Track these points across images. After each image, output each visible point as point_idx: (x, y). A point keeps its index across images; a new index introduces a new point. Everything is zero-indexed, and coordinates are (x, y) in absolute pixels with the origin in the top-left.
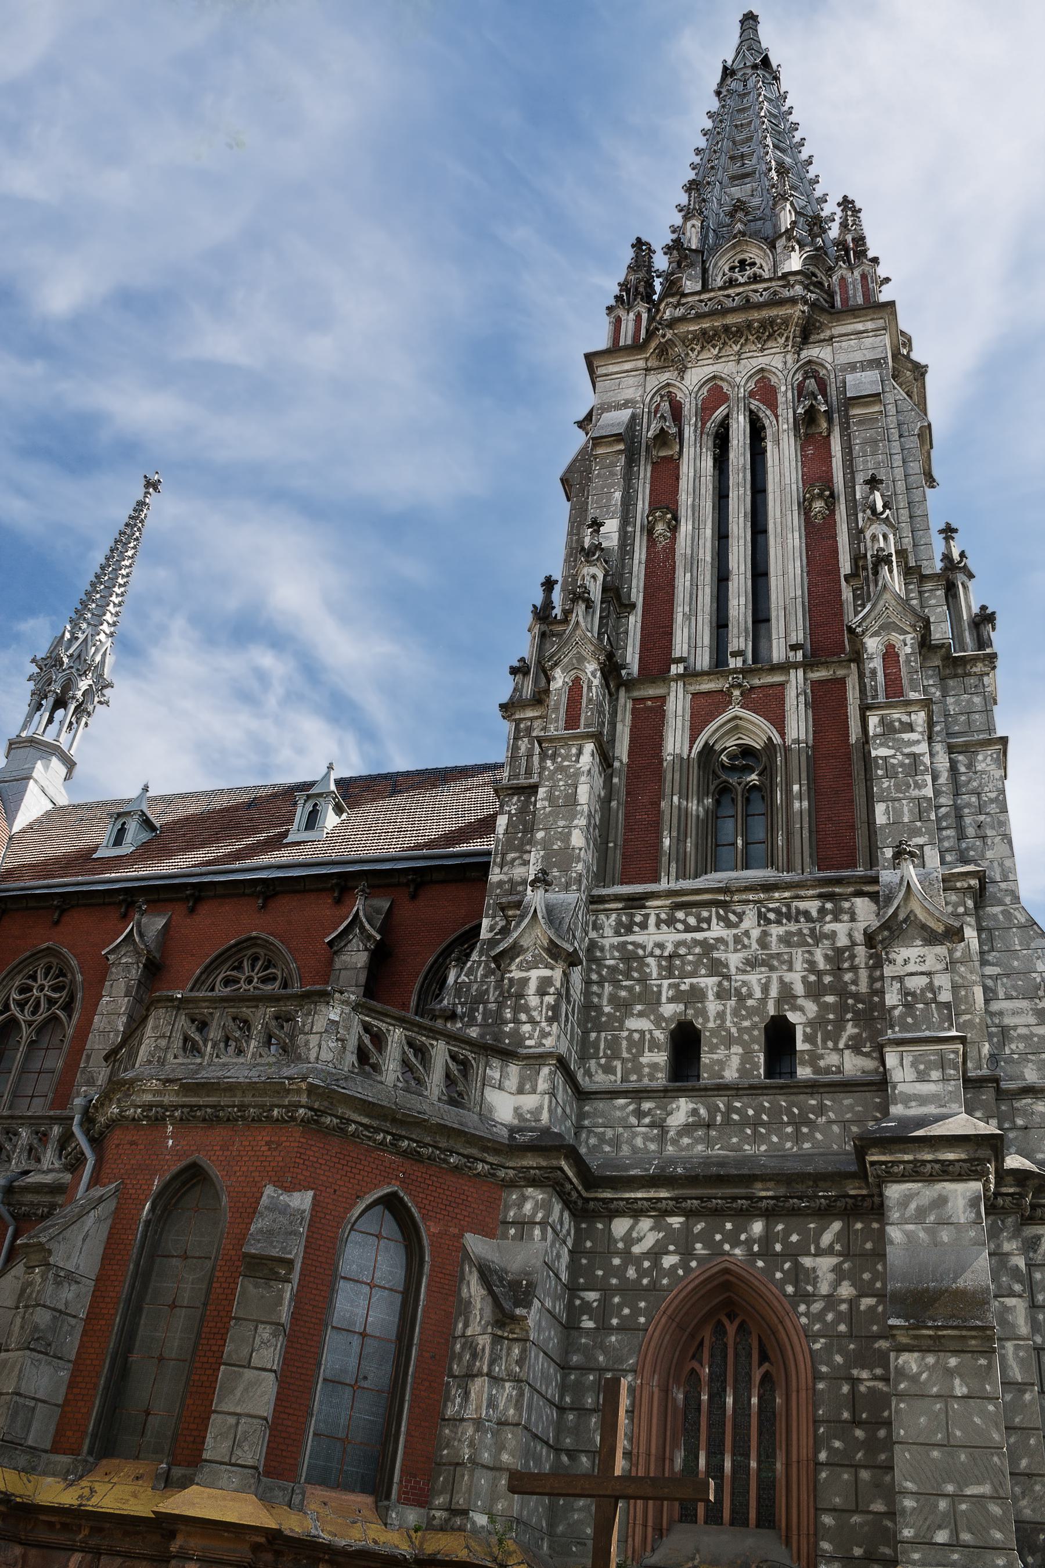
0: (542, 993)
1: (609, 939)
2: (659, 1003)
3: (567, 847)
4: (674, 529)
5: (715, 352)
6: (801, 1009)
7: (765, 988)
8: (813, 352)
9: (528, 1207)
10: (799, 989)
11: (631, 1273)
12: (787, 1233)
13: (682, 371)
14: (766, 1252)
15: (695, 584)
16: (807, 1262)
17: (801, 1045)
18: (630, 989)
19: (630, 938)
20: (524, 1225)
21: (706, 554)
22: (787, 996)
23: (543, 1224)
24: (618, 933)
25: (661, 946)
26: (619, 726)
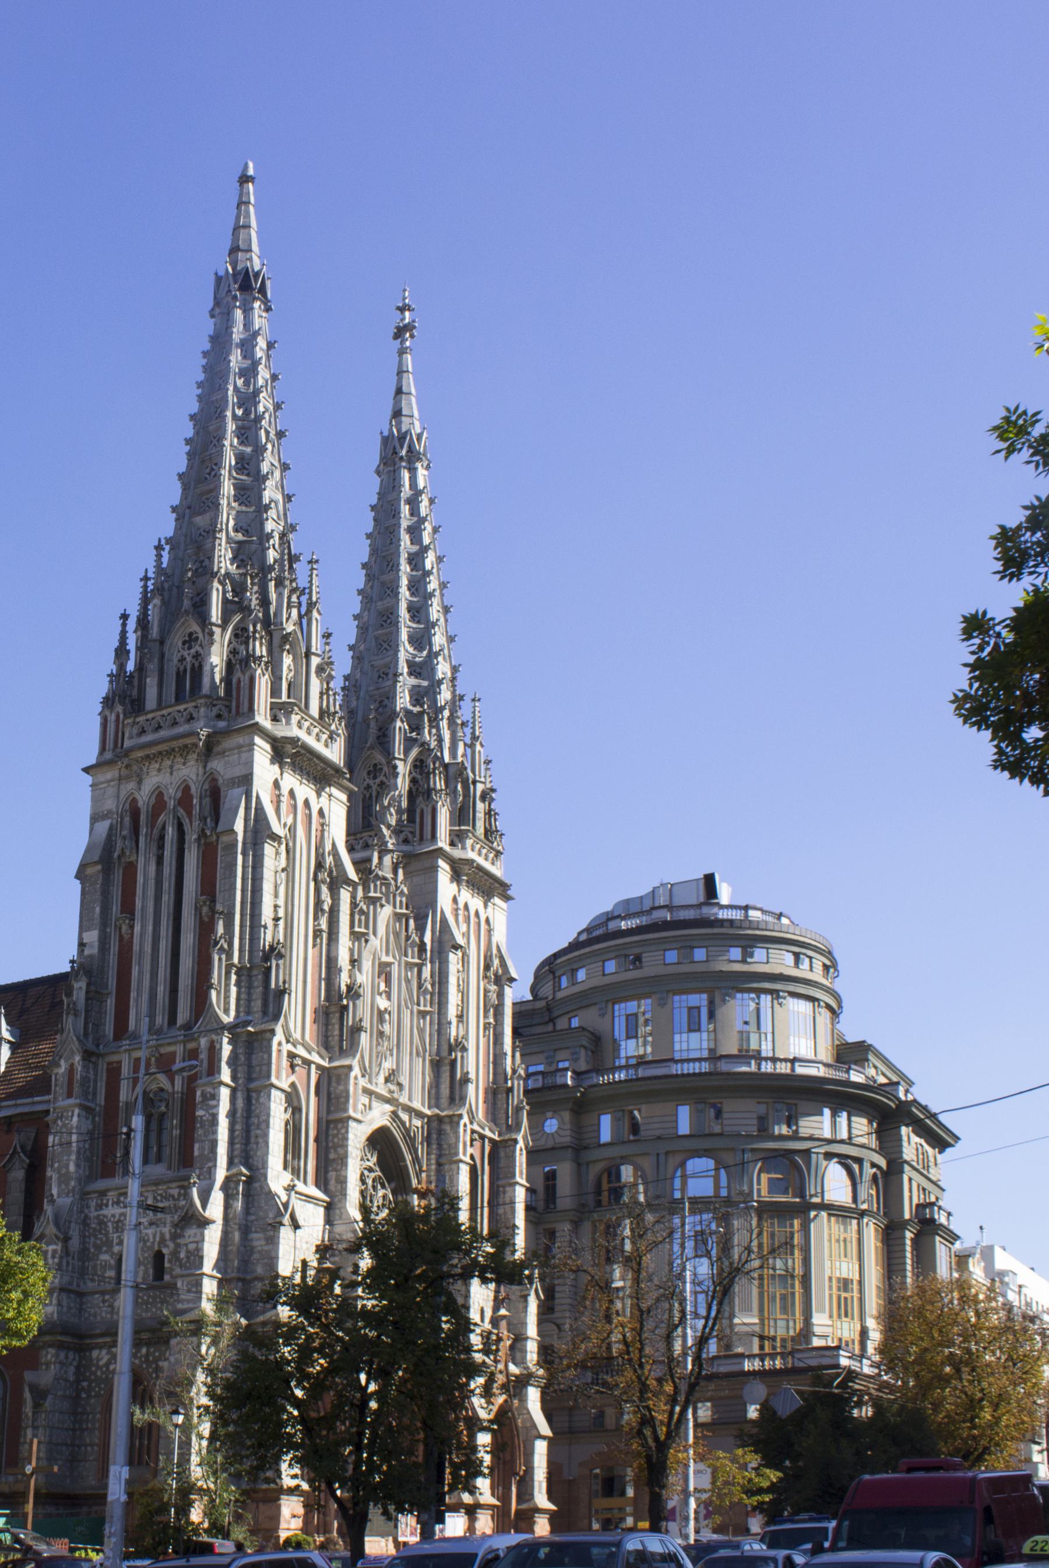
0: (53, 1257)
1: (93, 1214)
2: (112, 1246)
3: (68, 1172)
4: (132, 927)
5: (157, 766)
6: (167, 1246)
7: (154, 1237)
8: (216, 764)
9: (49, 1356)
10: (167, 1236)
11: (99, 1373)
12: (155, 1352)
13: (140, 782)
14: (147, 1361)
15: (141, 972)
16: (161, 1364)
17: (167, 1265)
18: (101, 1239)
19: (102, 1212)
20: (48, 1364)
21: (148, 948)
22: (163, 1240)
23: (55, 1363)
24: (96, 1210)
25: (113, 1216)
26: (99, 1084)
